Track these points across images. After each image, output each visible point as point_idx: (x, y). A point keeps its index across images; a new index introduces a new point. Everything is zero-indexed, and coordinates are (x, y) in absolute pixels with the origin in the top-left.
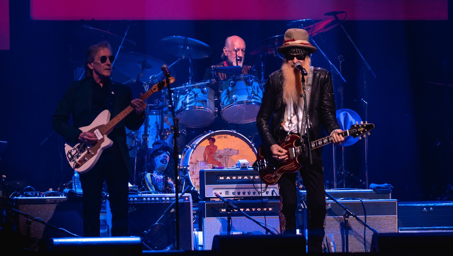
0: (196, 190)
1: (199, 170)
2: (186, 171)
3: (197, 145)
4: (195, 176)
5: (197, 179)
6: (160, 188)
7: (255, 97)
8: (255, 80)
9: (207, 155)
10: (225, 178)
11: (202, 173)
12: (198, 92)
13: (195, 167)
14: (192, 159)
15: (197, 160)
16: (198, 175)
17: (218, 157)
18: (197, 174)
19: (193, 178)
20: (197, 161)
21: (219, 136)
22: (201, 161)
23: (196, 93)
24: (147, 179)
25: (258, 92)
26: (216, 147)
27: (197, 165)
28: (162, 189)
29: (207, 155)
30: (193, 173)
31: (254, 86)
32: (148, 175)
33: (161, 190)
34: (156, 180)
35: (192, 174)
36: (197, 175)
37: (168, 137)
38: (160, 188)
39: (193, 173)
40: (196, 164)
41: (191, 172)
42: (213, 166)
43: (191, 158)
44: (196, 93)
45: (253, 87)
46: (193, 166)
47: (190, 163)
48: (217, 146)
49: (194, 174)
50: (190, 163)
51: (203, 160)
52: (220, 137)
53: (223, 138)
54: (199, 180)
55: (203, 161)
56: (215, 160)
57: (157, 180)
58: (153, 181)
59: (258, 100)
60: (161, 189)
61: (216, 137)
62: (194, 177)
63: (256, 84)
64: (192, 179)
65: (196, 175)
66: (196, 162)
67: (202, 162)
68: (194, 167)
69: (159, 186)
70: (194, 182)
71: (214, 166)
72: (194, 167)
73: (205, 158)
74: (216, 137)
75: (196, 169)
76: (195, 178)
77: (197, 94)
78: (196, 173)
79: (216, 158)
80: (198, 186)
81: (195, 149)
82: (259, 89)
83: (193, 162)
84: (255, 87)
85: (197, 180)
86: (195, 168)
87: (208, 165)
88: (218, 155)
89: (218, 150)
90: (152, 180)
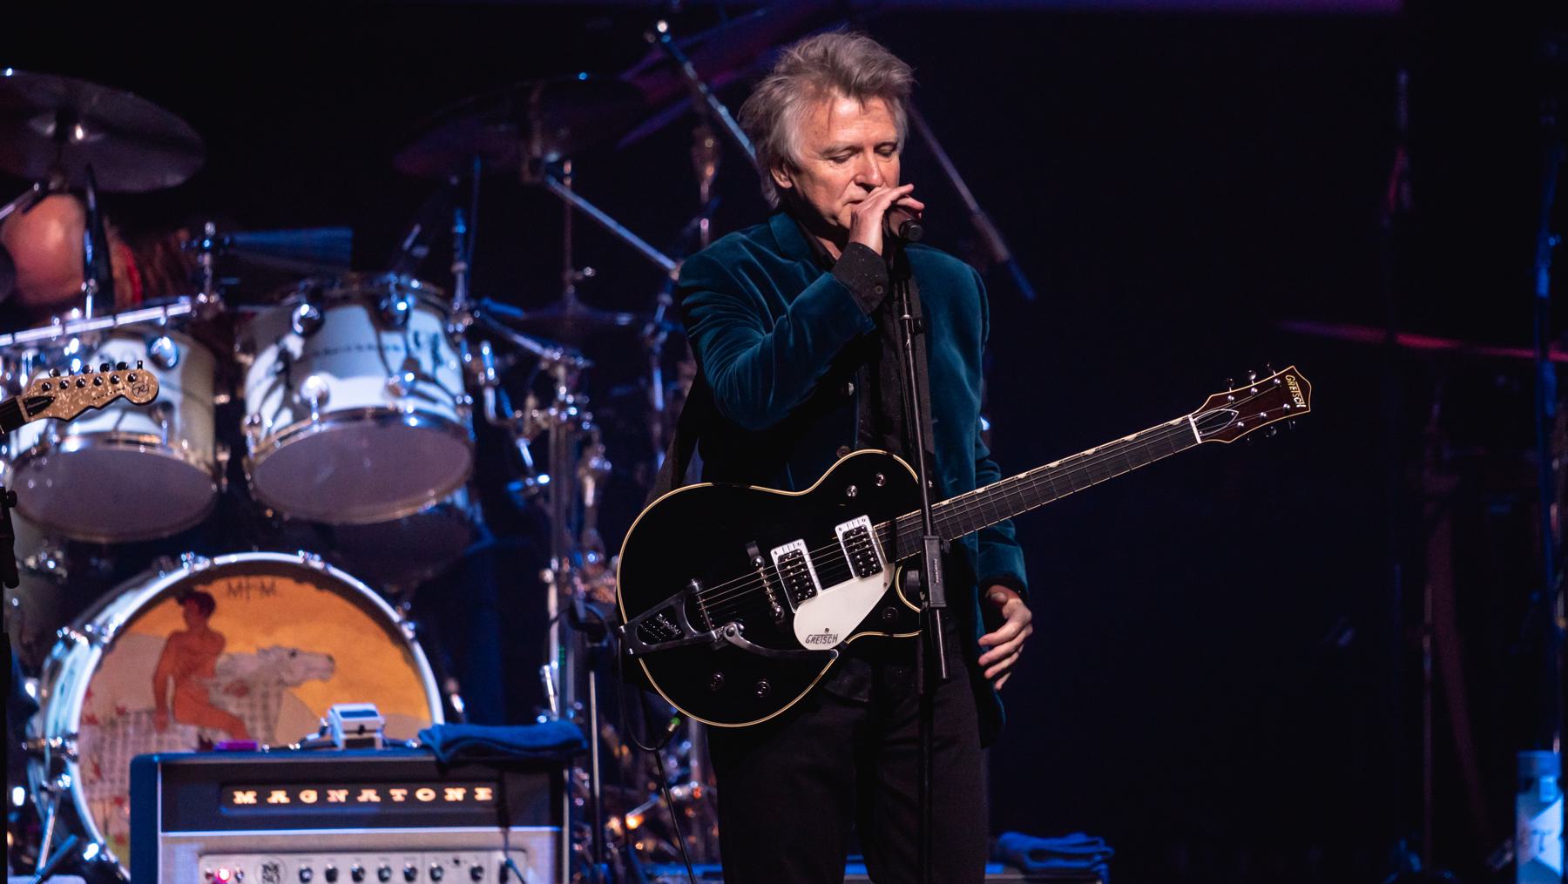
0: (113, 858)
1: (129, 758)
3: (121, 631)
4: (108, 785)
7: (422, 387)
8: (423, 303)
9: (171, 682)
10: (262, 798)
11: (142, 770)
14: (93, 699)
15: (120, 704)
16: (122, 781)
17: (227, 691)
18: (116, 775)
19: (96, 796)
20: (121, 712)
21: (234, 582)
22: (138, 714)
25: (437, 360)
26: (218, 642)
27: (120, 731)
29: (171, 682)
30: (97, 770)
31: (416, 336)
35: (91, 775)
36: (118, 784)
40: (113, 724)
41: (89, 766)
42: (201, 741)
45: (410, 337)
46: (98, 734)
48: (226, 634)
49: (104, 776)
50: (84, 718)
52: (240, 587)
53: (254, 593)
54: (127, 810)
55: (149, 713)
56: (212, 706)
59: (433, 400)
61: (217, 589)
62: (102, 790)
63: (425, 324)
64: (90, 801)
65: (112, 781)
66: (114, 715)
67: (144, 718)
68: (103, 740)
70: (100, 818)
71: (209, 734)
72: (103, 740)
73: (160, 694)
74: (217, 589)
75: (113, 751)
78: (112, 769)
79: (216, 696)
80: (119, 840)
82: (444, 350)
83: (99, 715)
84: (422, 339)
85: (116, 807)
86: (106, 745)
88: (226, 680)
89: (232, 657)
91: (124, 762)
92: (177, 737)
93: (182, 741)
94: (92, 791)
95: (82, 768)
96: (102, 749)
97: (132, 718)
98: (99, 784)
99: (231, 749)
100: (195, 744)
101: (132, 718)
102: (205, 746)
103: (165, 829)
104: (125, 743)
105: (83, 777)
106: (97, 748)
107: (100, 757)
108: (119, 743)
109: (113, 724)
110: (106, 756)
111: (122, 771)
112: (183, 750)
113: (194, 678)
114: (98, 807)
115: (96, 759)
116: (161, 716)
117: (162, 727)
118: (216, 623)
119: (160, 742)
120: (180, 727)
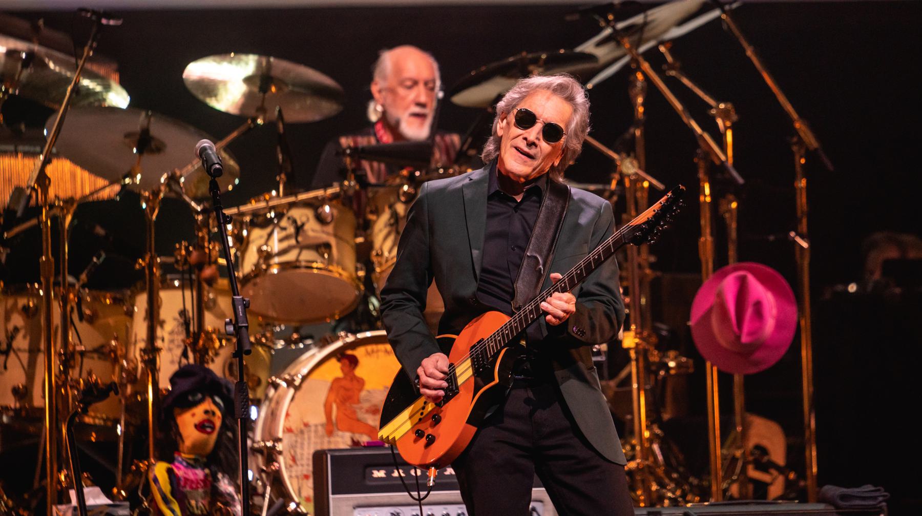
0: (304, 511)
1: (312, 451)
2: (270, 455)
3: (304, 378)
4: (300, 468)
5: (306, 477)
6: (195, 509)
9: (334, 407)
10: (389, 474)
11: (319, 457)
12: (304, 219)
13: (299, 440)
14: (290, 418)
15: (305, 421)
16: (308, 465)
17: (367, 411)
18: (305, 462)
19: (294, 474)
20: (306, 425)
21: (369, 348)
22: (316, 426)
23: (299, 223)
24: (156, 480)
26: (361, 382)
27: (306, 436)
28: (202, 511)
29: (334, 407)
30: (294, 459)
32: (160, 470)
33: (200, 512)
34: (182, 483)
35: (291, 462)
36: (306, 467)
37: (217, 354)
38: (195, 509)
39: (294, 459)
40: (302, 432)
41: (289, 457)
42: (353, 441)
43: (287, 415)
44: (299, 223)
46: (294, 438)
47: (284, 431)
48: (365, 378)
49: (298, 463)
50: (285, 429)
51: (323, 419)
52: (373, 351)
53: (381, 354)
55: (322, 425)
56: (358, 420)
57: (185, 483)
58: (175, 485)
60: (197, 508)
61: (359, 352)
62: (296, 471)
64: (290, 477)
65: (302, 465)
66: (302, 427)
67: (320, 428)
68: (296, 441)
69: (193, 503)
70: (296, 487)
71: (357, 437)
72: (296, 441)
73: (328, 414)
74: (359, 352)
75: (302, 448)
76: (299, 473)
77: (303, 225)
78: (302, 459)
79: (362, 415)
80: (308, 500)
81: (297, 388)
83: (293, 428)
85: (305, 481)
86: (299, 445)
87: (338, 436)
88: (366, 405)
89: (369, 391)
90: (171, 483)
91: (309, 454)
92: (339, 439)
93: (342, 441)
94: (291, 471)
95: (285, 458)
96: (296, 447)
97: (313, 429)
98: (295, 468)
99: (369, 446)
100: (349, 442)
101: (313, 429)
102: (356, 444)
103: (333, 494)
104: (309, 444)
105: (285, 463)
106: (293, 447)
107: (295, 452)
108: (306, 443)
109: (302, 432)
110: (299, 451)
111: (308, 459)
112: (342, 446)
113: (348, 404)
114: (295, 481)
115: (292, 452)
116: (330, 428)
117: (330, 433)
118: (359, 372)
119: (329, 442)
120: (340, 433)
